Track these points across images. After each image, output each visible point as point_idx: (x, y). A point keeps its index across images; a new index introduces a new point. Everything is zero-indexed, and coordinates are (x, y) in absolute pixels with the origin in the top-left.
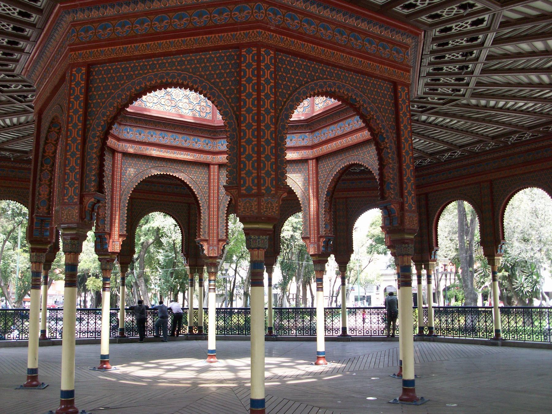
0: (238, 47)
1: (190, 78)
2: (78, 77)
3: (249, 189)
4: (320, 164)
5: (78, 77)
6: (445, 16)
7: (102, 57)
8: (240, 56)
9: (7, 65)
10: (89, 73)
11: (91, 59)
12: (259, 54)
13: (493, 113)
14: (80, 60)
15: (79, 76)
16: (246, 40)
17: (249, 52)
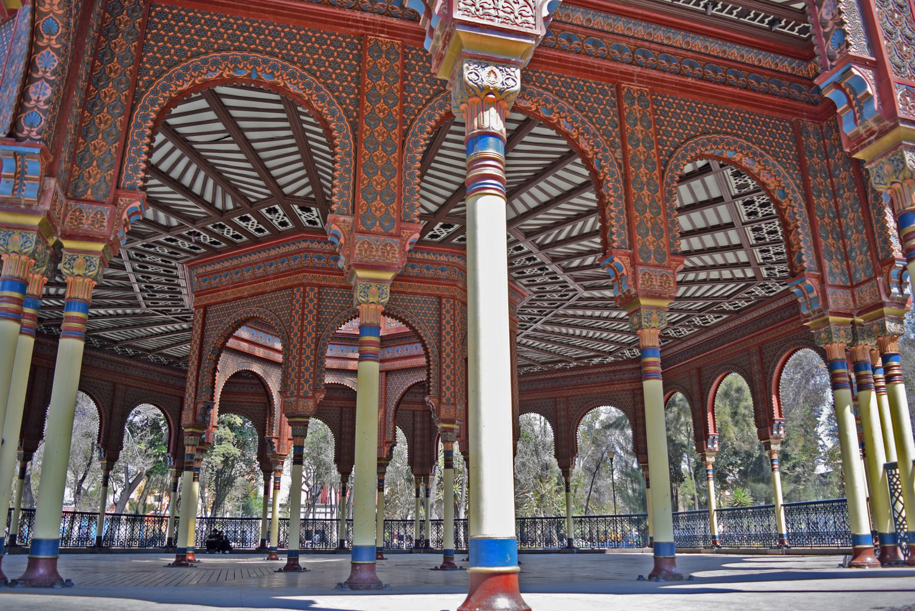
0: (440, 298)
1: (403, 312)
2: (312, 295)
3: (448, 400)
4: (390, 377)
5: (312, 295)
6: (548, 289)
7: (334, 283)
8: (440, 303)
9: (176, 254)
10: (319, 293)
11: (323, 283)
12: (454, 304)
13: (525, 349)
14: (315, 282)
15: (312, 294)
16: (446, 293)
17: (448, 302)
